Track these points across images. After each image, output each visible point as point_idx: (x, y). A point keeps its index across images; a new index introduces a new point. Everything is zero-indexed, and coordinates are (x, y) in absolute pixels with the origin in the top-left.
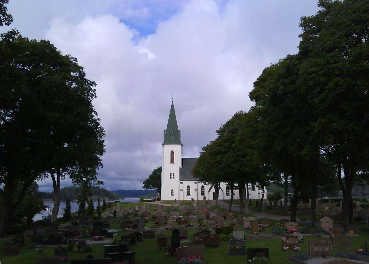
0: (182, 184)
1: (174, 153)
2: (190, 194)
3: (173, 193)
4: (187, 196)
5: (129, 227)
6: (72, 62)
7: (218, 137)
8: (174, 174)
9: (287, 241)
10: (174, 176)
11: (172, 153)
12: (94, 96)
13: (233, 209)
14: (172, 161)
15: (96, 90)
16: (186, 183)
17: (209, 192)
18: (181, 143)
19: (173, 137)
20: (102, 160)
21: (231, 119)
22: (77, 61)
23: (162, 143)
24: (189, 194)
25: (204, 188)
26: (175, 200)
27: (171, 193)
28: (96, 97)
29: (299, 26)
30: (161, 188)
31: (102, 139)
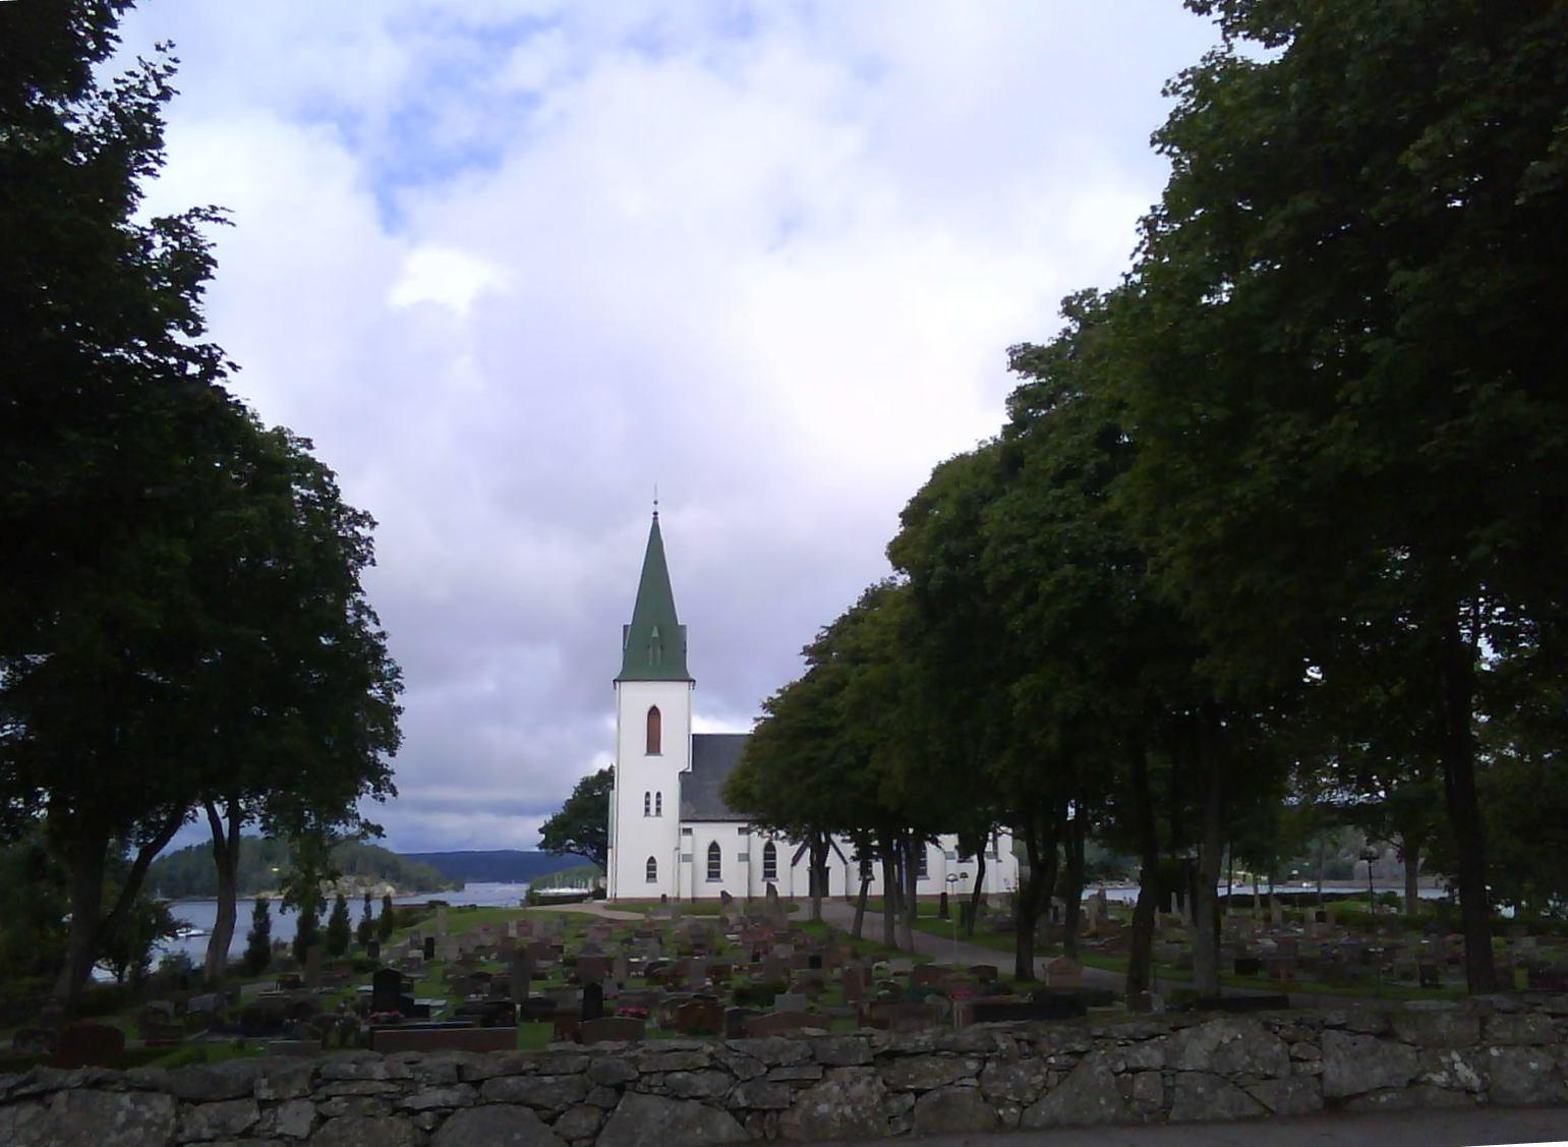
3: (654, 869)
4: (707, 881)
6: (295, 452)
7: (808, 671)
8: (659, 795)
10: (658, 803)
11: (654, 713)
12: (368, 561)
13: (865, 932)
14: (653, 746)
15: (373, 541)
16: (705, 833)
17: (794, 868)
20: (393, 773)
22: (310, 447)
23: (615, 677)
24: (718, 875)
25: (774, 850)
26: (664, 896)
27: (649, 868)
28: (373, 563)
29: (1009, 370)
30: (609, 851)
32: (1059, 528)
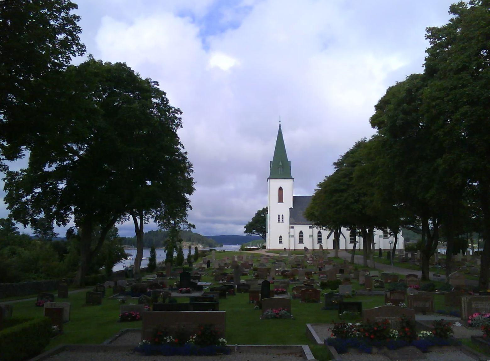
0: (293, 229)
1: (282, 190)
3: (282, 239)
5: (223, 280)
6: (153, 86)
7: (335, 171)
8: (283, 216)
10: (283, 218)
11: (281, 189)
12: (180, 126)
13: (355, 261)
14: (281, 200)
15: (181, 119)
16: (298, 228)
17: (328, 240)
18: (291, 177)
20: (190, 201)
21: (352, 148)
22: (158, 85)
23: (268, 178)
24: (302, 242)
25: (321, 233)
26: (285, 248)
27: (280, 239)
28: (182, 127)
30: (267, 233)
31: (190, 176)
32: (461, 91)
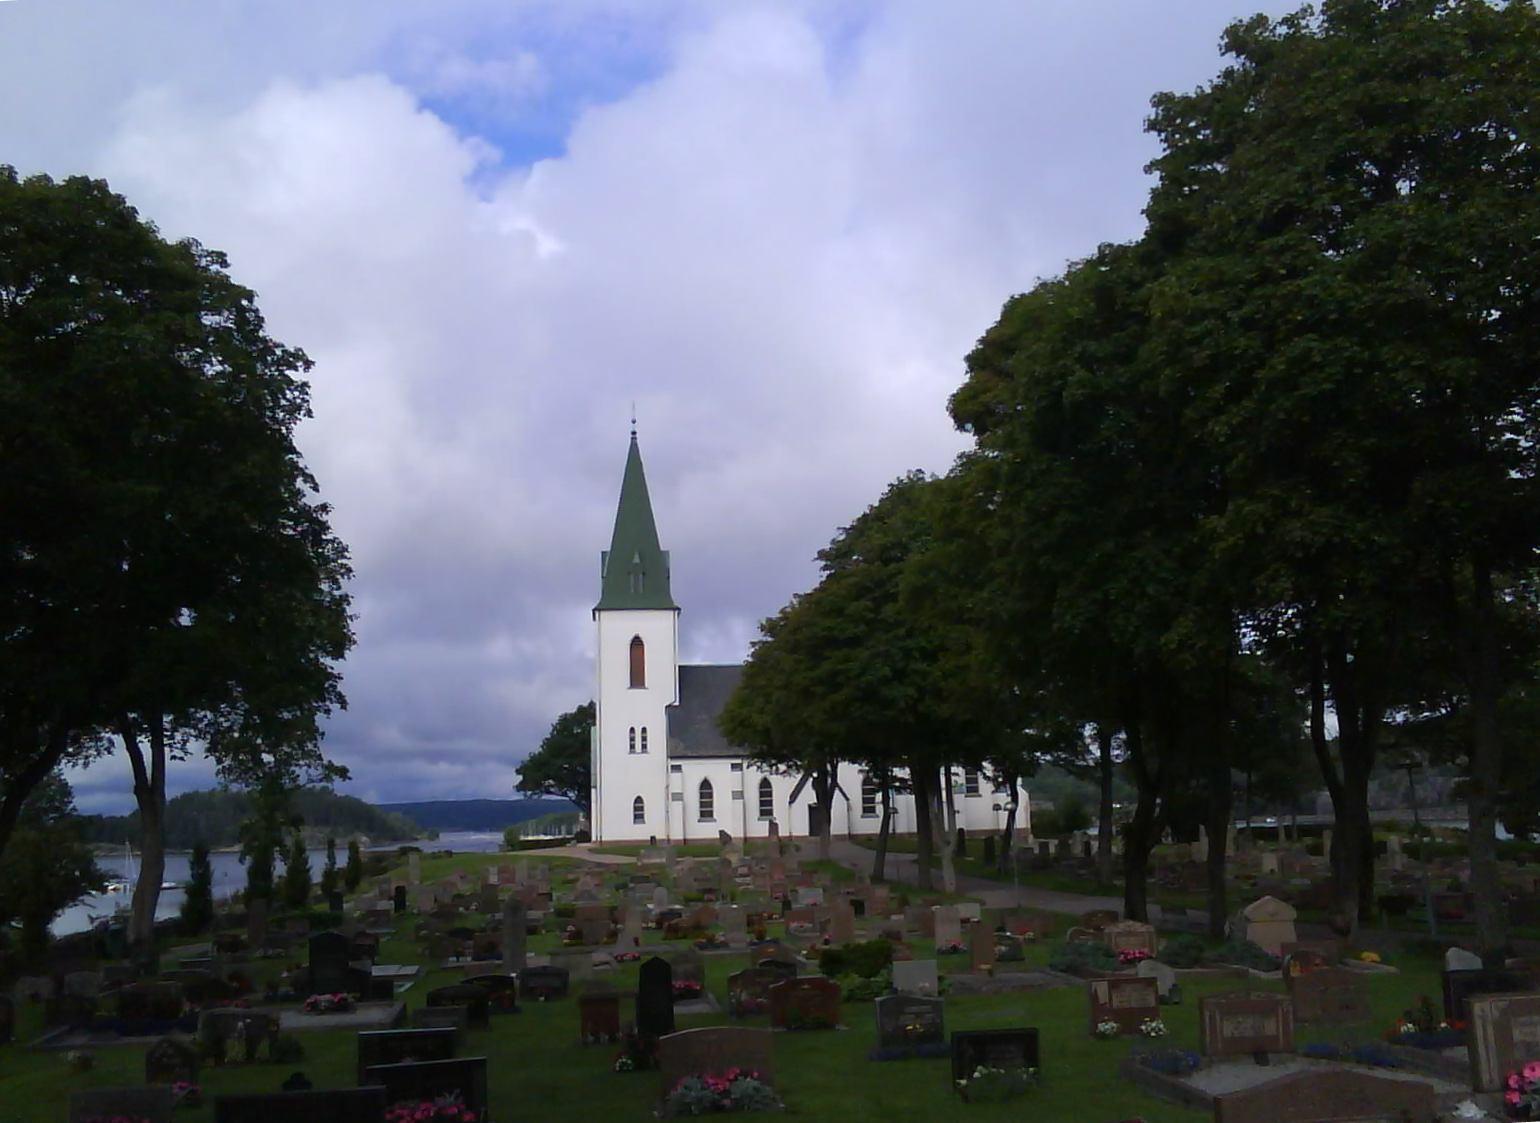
0: (680, 774)
1: (641, 642)
2: (711, 812)
3: (642, 809)
6: (206, 269)
7: (824, 579)
8: (644, 730)
9: (1111, 999)
10: (644, 739)
11: (637, 644)
12: (302, 412)
13: (889, 872)
14: (637, 679)
15: (309, 387)
16: (696, 771)
17: (793, 805)
19: (641, 583)
22: (224, 264)
23: (593, 607)
24: (710, 814)
25: (770, 787)
26: (653, 838)
27: (636, 809)
28: (309, 413)
30: (593, 791)
31: (339, 588)
32: (1289, 287)
